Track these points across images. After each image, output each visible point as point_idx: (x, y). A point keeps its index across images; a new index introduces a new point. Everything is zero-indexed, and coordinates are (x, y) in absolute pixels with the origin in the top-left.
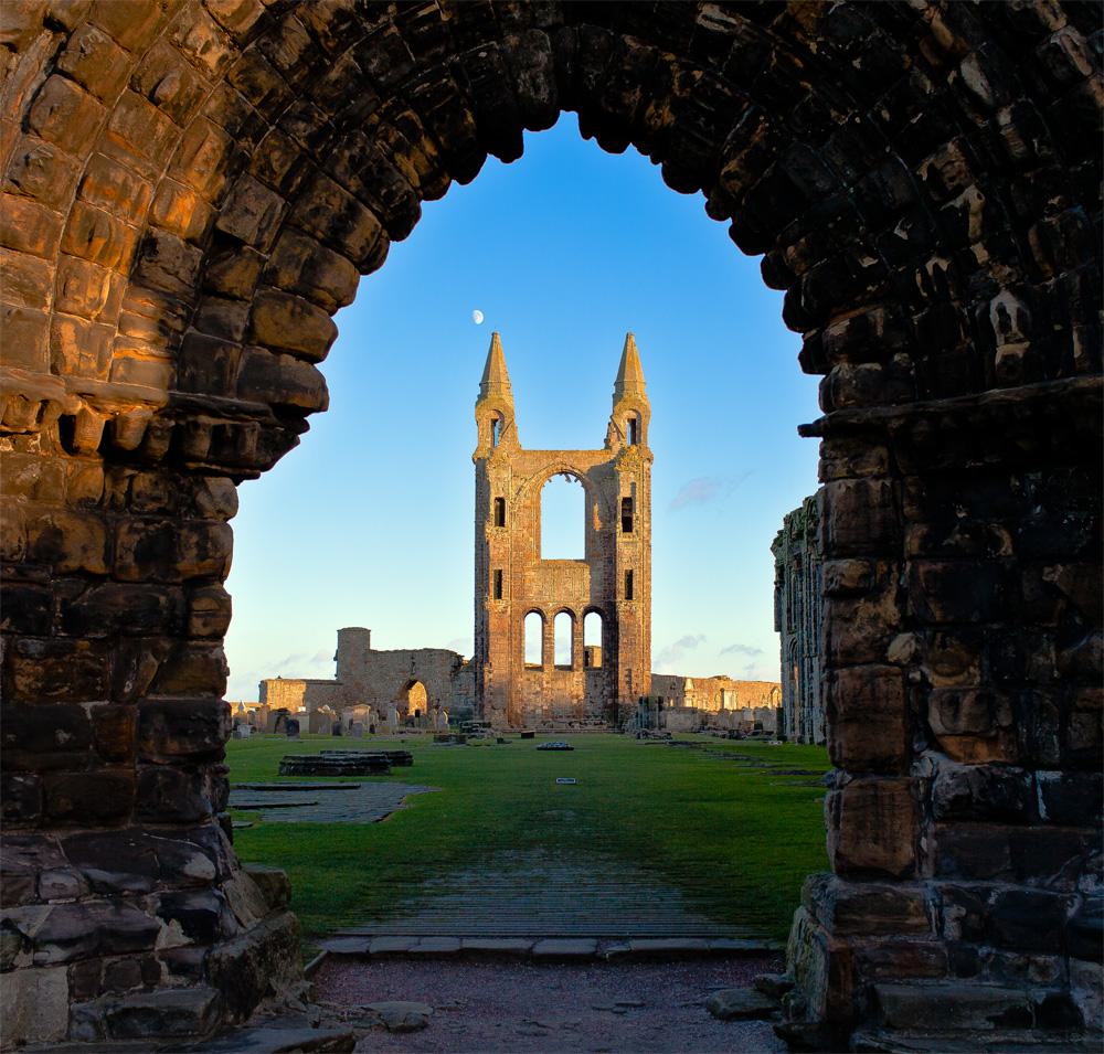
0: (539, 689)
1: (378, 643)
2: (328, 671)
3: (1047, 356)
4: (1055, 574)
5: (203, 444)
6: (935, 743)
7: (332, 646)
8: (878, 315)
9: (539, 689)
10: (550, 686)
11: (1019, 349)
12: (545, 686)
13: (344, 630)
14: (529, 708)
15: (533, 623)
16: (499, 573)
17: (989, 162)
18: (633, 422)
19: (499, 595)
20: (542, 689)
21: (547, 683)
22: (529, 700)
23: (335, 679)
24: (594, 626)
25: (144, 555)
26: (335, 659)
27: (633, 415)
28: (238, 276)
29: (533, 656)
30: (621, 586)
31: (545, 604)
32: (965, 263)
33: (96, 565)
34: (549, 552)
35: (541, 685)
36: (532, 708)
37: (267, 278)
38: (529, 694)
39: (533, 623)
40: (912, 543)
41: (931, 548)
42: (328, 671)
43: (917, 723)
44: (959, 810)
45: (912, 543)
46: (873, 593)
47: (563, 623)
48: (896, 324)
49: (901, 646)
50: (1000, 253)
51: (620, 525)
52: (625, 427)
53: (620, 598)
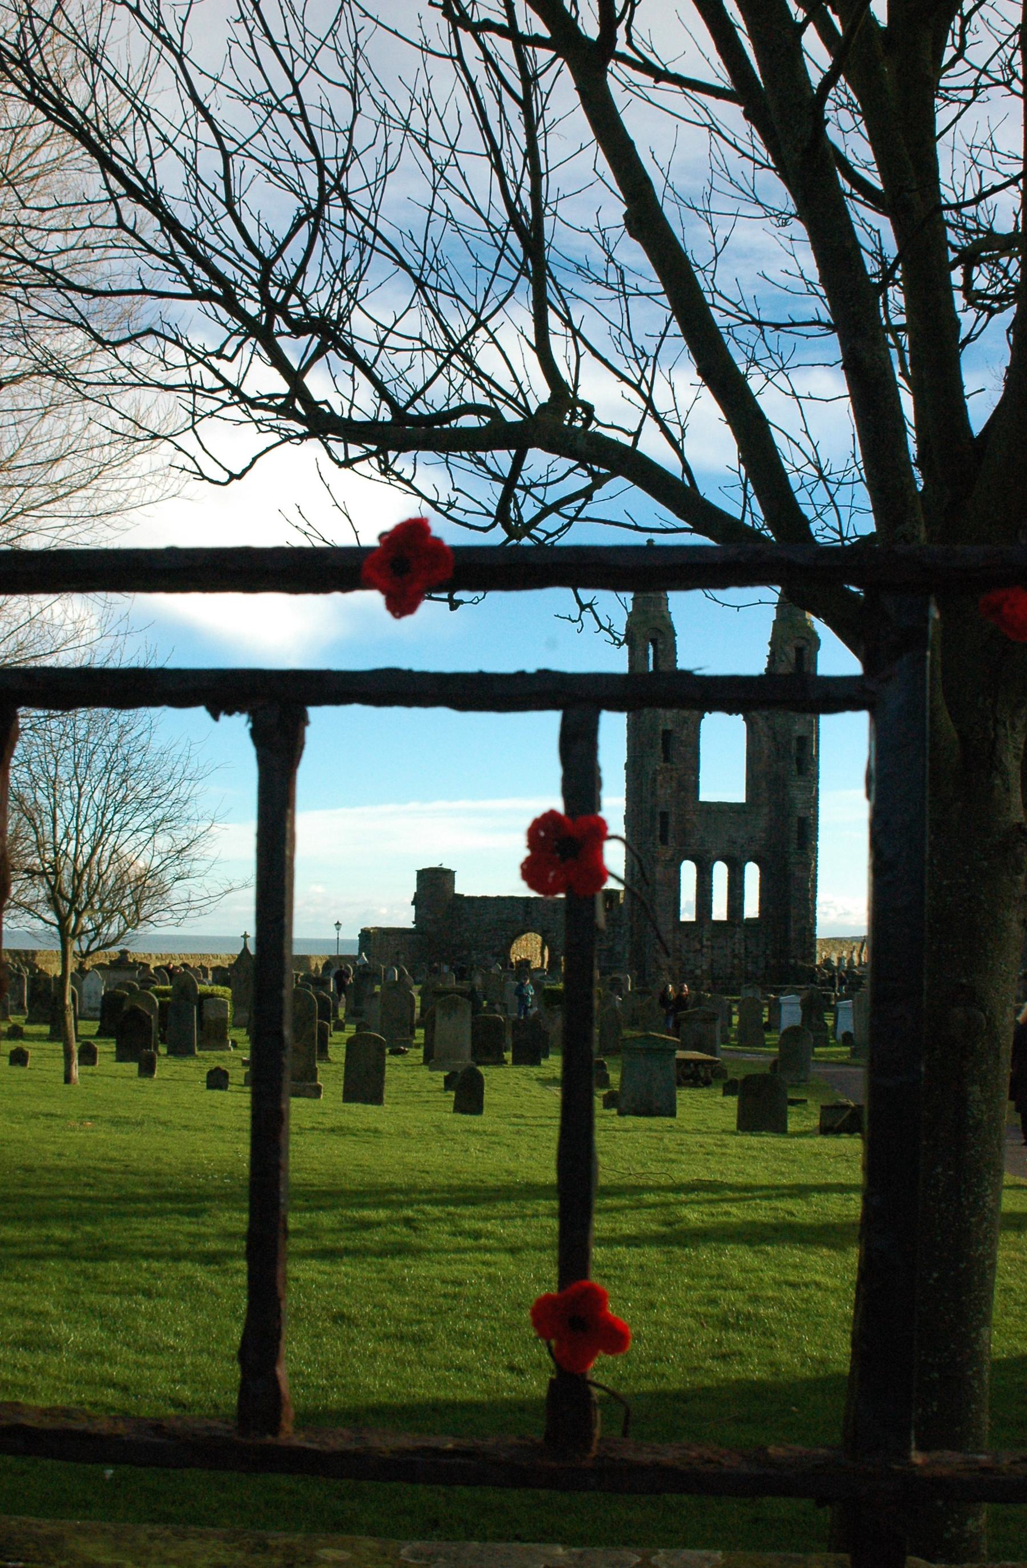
0: (698, 947)
1: (465, 886)
2: (405, 917)
7: (411, 888)
9: (698, 947)
10: (709, 943)
12: (705, 943)
13: (424, 870)
14: (688, 968)
15: (688, 871)
16: (664, 815)
18: (799, 651)
19: (664, 839)
20: (703, 946)
21: (708, 940)
22: (688, 959)
23: (413, 926)
24: (752, 872)
26: (413, 903)
27: (801, 643)
29: (688, 913)
30: (794, 835)
31: (707, 852)
34: (706, 795)
35: (701, 942)
36: (692, 967)
38: (687, 952)
39: (688, 871)
42: (405, 917)
47: (720, 871)
51: (794, 767)
52: (792, 655)
53: (793, 847)
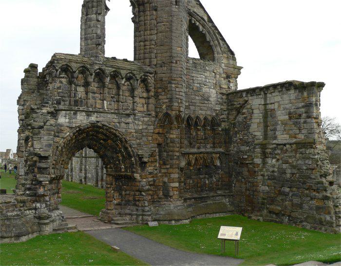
3: (126, 171)
4: (125, 187)
6: (115, 199)
8: (112, 166)
11: (124, 170)
17: (123, 156)
32: (120, 163)
37: (65, 163)
40: (114, 184)
41: (115, 184)
43: (113, 197)
44: (117, 204)
45: (114, 184)
46: (110, 188)
48: (114, 166)
49: (112, 192)
50: (123, 162)
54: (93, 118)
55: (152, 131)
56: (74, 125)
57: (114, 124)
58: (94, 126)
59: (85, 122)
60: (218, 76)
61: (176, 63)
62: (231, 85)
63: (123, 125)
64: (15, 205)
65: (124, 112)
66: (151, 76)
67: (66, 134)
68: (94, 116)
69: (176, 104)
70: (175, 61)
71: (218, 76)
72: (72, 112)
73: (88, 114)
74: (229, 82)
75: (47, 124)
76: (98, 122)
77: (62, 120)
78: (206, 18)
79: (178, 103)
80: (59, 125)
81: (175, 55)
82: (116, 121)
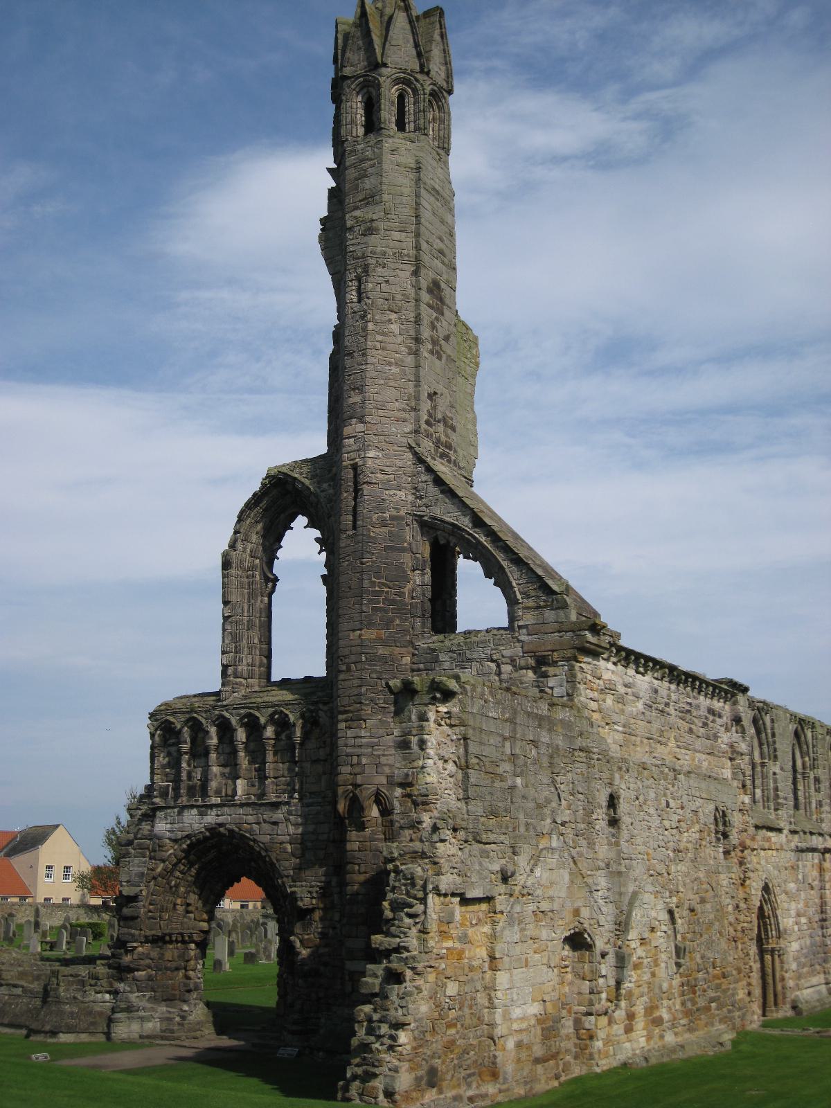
5: (187, 938)
25: (179, 957)
28: (190, 908)
33: (170, 959)
54: (211, 818)
55: (325, 836)
56: (180, 835)
57: (249, 826)
58: (213, 830)
59: (196, 826)
60: (507, 668)
61: (349, 670)
62: (552, 682)
63: (266, 827)
64: (83, 981)
65: (279, 797)
66: (325, 708)
67: (167, 851)
68: (212, 813)
69: (345, 769)
70: (344, 668)
71: (507, 668)
72: (176, 810)
73: (204, 809)
74: (545, 675)
75: (139, 836)
76: (221, 825)
77: (161, 827)
78: (465, 522)
79: (352, 765)
80: (155, 835)
81: (346, 651)
82: (251, 819)
